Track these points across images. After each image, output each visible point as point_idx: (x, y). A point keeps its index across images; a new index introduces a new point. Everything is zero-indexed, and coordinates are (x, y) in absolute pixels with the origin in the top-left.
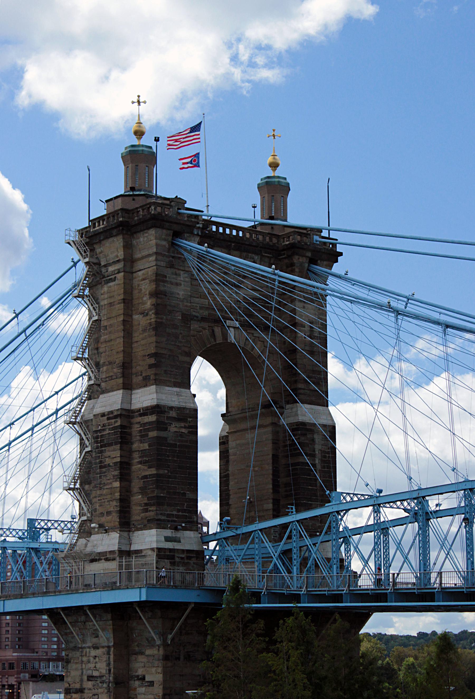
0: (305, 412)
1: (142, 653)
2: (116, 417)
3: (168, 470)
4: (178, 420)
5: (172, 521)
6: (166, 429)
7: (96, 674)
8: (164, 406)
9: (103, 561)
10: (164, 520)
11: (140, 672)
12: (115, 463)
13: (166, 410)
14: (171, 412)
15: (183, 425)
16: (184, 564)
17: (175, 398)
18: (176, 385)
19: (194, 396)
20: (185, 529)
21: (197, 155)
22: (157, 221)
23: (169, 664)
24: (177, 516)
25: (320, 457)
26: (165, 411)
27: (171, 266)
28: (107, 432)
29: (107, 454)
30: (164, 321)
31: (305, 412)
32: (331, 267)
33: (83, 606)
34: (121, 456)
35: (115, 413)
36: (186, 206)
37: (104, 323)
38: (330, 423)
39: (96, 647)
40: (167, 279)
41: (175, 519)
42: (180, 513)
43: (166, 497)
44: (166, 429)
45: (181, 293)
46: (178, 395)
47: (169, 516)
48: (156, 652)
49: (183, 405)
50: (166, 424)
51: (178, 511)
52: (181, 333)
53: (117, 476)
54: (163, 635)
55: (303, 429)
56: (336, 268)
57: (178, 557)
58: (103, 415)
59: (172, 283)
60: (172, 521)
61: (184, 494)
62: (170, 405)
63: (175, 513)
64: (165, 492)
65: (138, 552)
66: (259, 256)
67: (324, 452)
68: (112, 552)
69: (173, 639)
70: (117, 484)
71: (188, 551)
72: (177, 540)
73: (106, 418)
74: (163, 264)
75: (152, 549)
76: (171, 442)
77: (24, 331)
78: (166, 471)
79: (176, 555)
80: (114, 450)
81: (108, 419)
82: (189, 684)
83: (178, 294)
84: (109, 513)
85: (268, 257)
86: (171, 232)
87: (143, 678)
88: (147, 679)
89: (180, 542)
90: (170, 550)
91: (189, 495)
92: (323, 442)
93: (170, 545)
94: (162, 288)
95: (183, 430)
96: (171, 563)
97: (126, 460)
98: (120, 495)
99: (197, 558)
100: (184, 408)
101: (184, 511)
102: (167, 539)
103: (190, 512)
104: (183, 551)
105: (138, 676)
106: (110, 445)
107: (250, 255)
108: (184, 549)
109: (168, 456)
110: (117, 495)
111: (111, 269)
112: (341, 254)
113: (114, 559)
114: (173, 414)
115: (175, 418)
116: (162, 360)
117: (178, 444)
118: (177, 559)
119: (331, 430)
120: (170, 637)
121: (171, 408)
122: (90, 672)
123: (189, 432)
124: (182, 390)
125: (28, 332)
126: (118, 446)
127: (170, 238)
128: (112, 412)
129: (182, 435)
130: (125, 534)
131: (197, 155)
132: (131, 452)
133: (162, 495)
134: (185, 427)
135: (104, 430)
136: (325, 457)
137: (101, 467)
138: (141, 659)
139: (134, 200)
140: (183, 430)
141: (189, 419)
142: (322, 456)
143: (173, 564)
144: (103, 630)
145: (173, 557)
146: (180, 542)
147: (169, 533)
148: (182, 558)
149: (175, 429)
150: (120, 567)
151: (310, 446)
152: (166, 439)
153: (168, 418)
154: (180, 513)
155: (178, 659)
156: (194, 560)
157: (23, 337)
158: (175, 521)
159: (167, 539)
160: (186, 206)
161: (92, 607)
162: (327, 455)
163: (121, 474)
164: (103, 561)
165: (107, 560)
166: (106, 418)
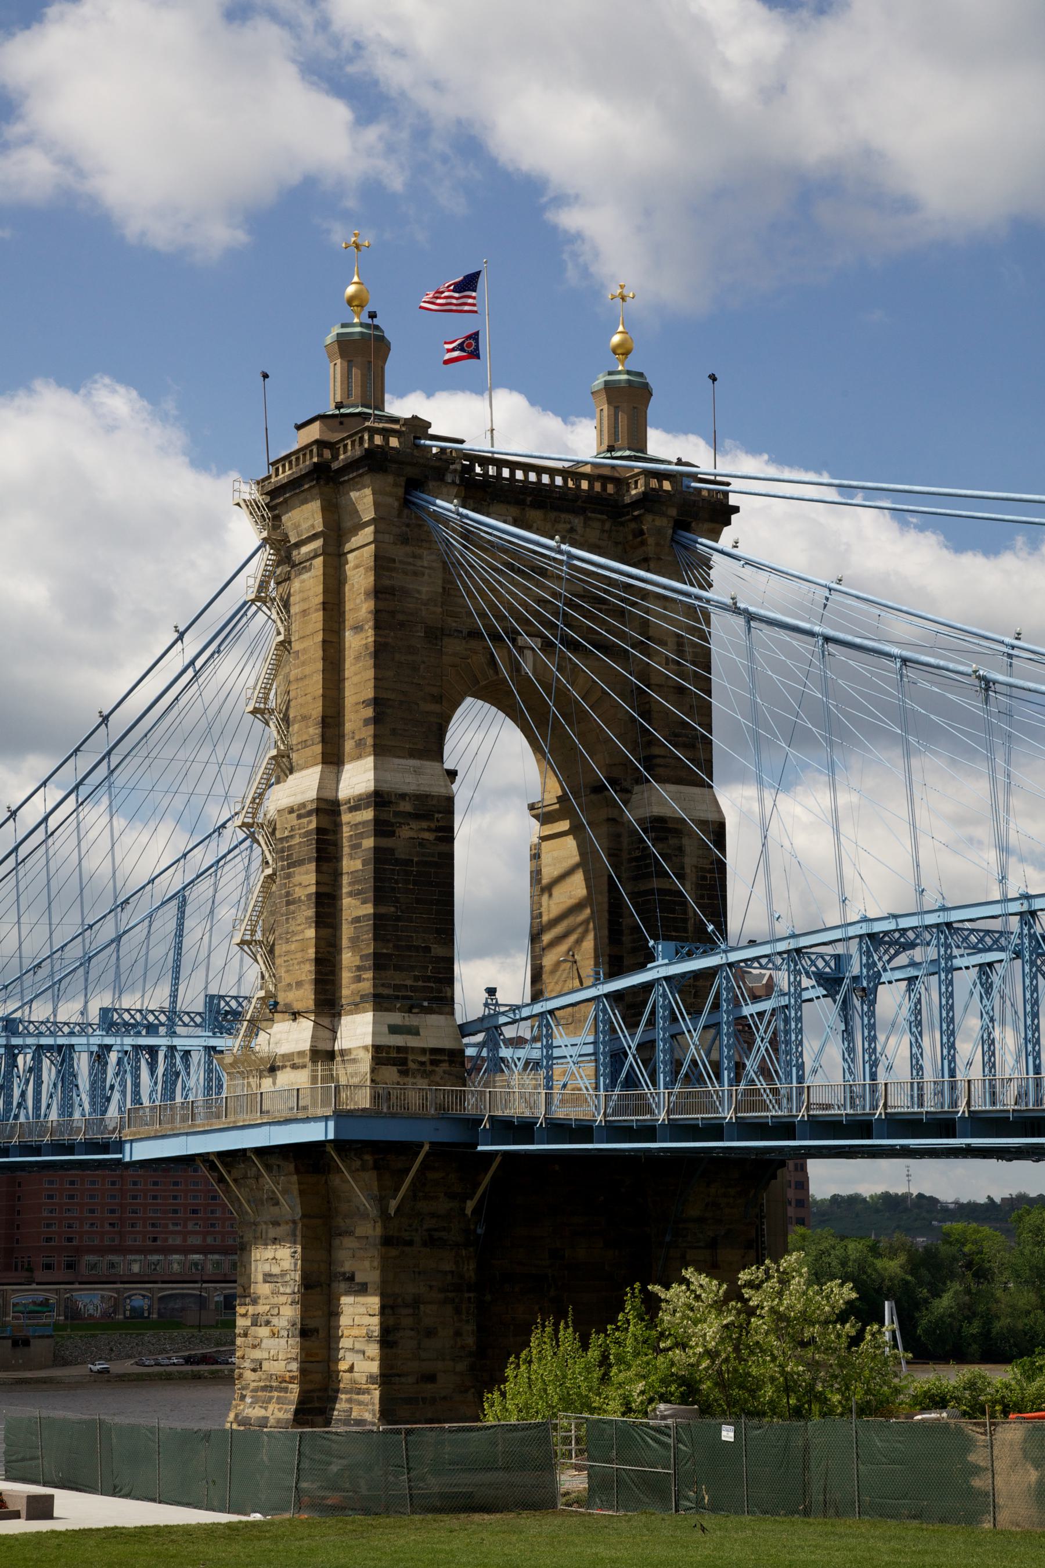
0: (666, 799)
1: (350, 1233)
2: (309, 814)
3: (396, 907)
4: (417, 816)
5: (405, 998)
6: (392, 834)
7: (276, 1270)
8: (389, 793)
9: (288, 1069)
10: (388, 997)
11: (347, 1267)
12: (309, 896)
13: (393, 799)
14: (402, 804)
15: (425, 825)
16: (426, 1074)
17: (410, 778)
18: (414, 754)
19: (452, 774)
20: (429, 1011)
21: (475, 336)
22: (375, 461)
23: (394, 1252)
24: (413, 989)
25: (694, 879)
26: (390, 802)
27: (404, 540)
28: (297, 840)
29: (297, 879)
30: (390, 640)
31: (666, 799)
32: (715, 536)
33: (244, 1150)
34: (318, 883)
35: (309, 808)
36: (431, 431)
37: (296, 646)
38: (711, 816)
39: (276, 1224)
40: (397, 565)
41: (409, 993)
42: (420, 983)
43: (392, 955)
44: (392, 834)
45: (424, 589)
46: (417, 772)
47: (397, 987)
48: (370, 1229)
49: (425, 789)
50: (392, 825)
51: (416, 979)
52: (424, 662)
53: (311, 918)
54: (381, 1202)
55: (663, 828)
56: (727, 537)
57: (413, 1061)
58: (291, 811)
59: (405, 573)
60: (405, 998)
61: (427, 949)
62: (400, 791)
63: (409, 982)
64: (391, 945)
65: (343, 1053)
66: (582, 518)
67: (702, 869)
68: (301, 1054)
69: (398, 1209)
70: (311, 933)
71: (434, 1051)
72: (414, 1031)
73: (295, 815)
74: (387, 538)
75: (366, 1048)
76: (403, 857)
77: (192, 663)
78: (392, 909)
79: (410, 1057)
80: (306, 873)
81: (299, 817)
82: (431, 1287)
83: (419, 592)
84: (299, 984)
85: (599, 520)
86: (402, 480)
87: (351, 1278)
88: (359, 1278)
89: (417, 1034)
90: (399, 1049)
91: (437, 950)
93: (398, 1040)
94: (387, 582)
95: (426, 835)
96: (399, 1071)
97: (325, 889)
98: (316, 953)
99: (451, 1062)
100: (427, 796)
101: (427, 979)
102: (394, 1030)
103: (439, 981)
104: (423, 1051)
105: (344, 1274)
106: (300, 863)
107: (563, 516)
108: (425, 1046)
110: (311, 952)
111: (304, 550)
112: (736, 509)
113: (304, 1066)
114: (406, 807)
115: (409, 814)
116: (388, 711)
117: (415, 859)
118: (412, 1065)
119: (718, 832)
120: (393, 1204)
121: (403, 796)
122: (266, 1268)
123: (438, 839)
124: (427, 763)
125: (198, 664)
126: (313, 866)
127: (401, 491)
128: (303, 805)
129: (422, 843)
130: (326, 1021)
131: (475, 336)
132: (337, 874)
133: (385, 951)
134: (429, 830)
135: (292, 837)
137: (288, 903)
138: (349, 1242)
139: (341, 423)
140: (426, 835)
141: (436, 815)
143: (404, 1073)
144: (284, 1192)
145: (403, 1062)
146: (417, 1034)
147: (396, 1018)
148: (423, 1063)
149: (412, 834)
150: (314, 1079)
151: (674, 858)
152: (391, 851)
153: (397, 814)
154: (420, 983)
155: (410, 1243)
156: (445, 1066)
157: (190, 673)
158: (409, 998)
159: (394, 1030)
160: (431, 431)
161: (260, 1151)
163: (318, 915)
164: (288, 1069)
165: (294, 1067)
166: (295, 815)
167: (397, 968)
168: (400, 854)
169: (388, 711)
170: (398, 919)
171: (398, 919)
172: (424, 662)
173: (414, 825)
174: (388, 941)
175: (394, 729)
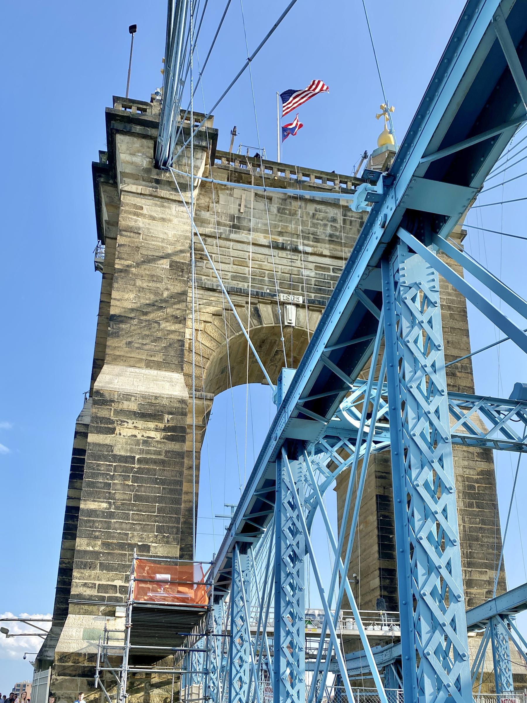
3: (110, 503)
4: (143, 416)
6: (112, 431)
15: (152, 425)
26: (113, 401)
41: (118, 595)
43: (100, 553)
44: (112, 431)
61: (145, 548)
64: (99, 543)
76: (123, 453)
78: (105, 505)
92: (466, 463)
95: (152, 434)
109: (112, 477)
114: (133, 406)
115: (135, 413)
117: (137, 457)
129: (147, 442)
134: (156, 429)
136: (472, 487)
142: (464, 486)
152: (110, 447)
153: (118, 412)
162: (476, 485)
167: (104, 567)
168: (119, 451)
169: (123, 326)
170: (111, 515)
171: (111, 515)
172: (167, 289)
173: (140, 424)
174: (96, 538)
175: (130, 343)
